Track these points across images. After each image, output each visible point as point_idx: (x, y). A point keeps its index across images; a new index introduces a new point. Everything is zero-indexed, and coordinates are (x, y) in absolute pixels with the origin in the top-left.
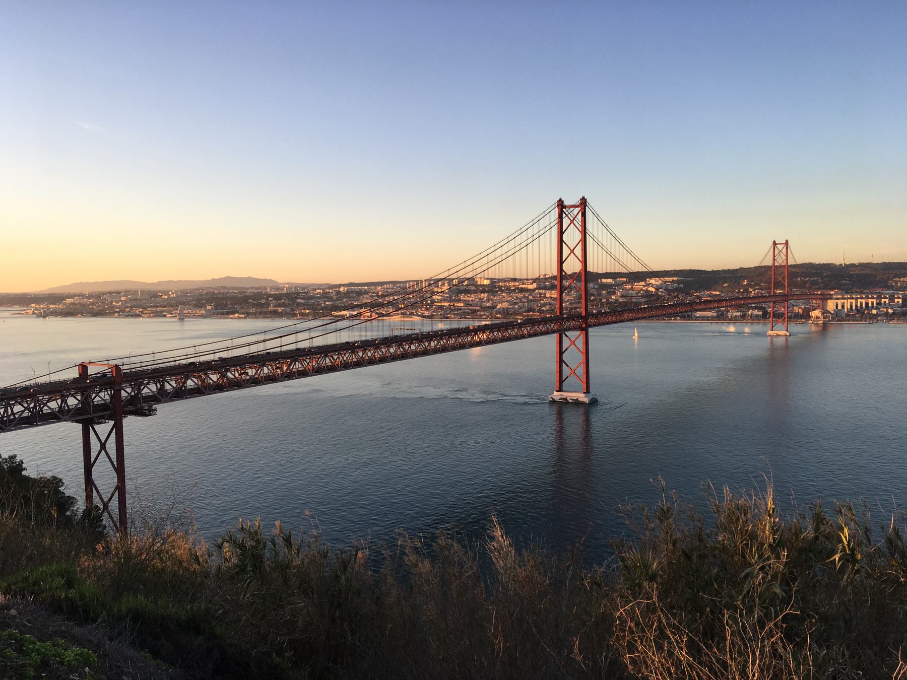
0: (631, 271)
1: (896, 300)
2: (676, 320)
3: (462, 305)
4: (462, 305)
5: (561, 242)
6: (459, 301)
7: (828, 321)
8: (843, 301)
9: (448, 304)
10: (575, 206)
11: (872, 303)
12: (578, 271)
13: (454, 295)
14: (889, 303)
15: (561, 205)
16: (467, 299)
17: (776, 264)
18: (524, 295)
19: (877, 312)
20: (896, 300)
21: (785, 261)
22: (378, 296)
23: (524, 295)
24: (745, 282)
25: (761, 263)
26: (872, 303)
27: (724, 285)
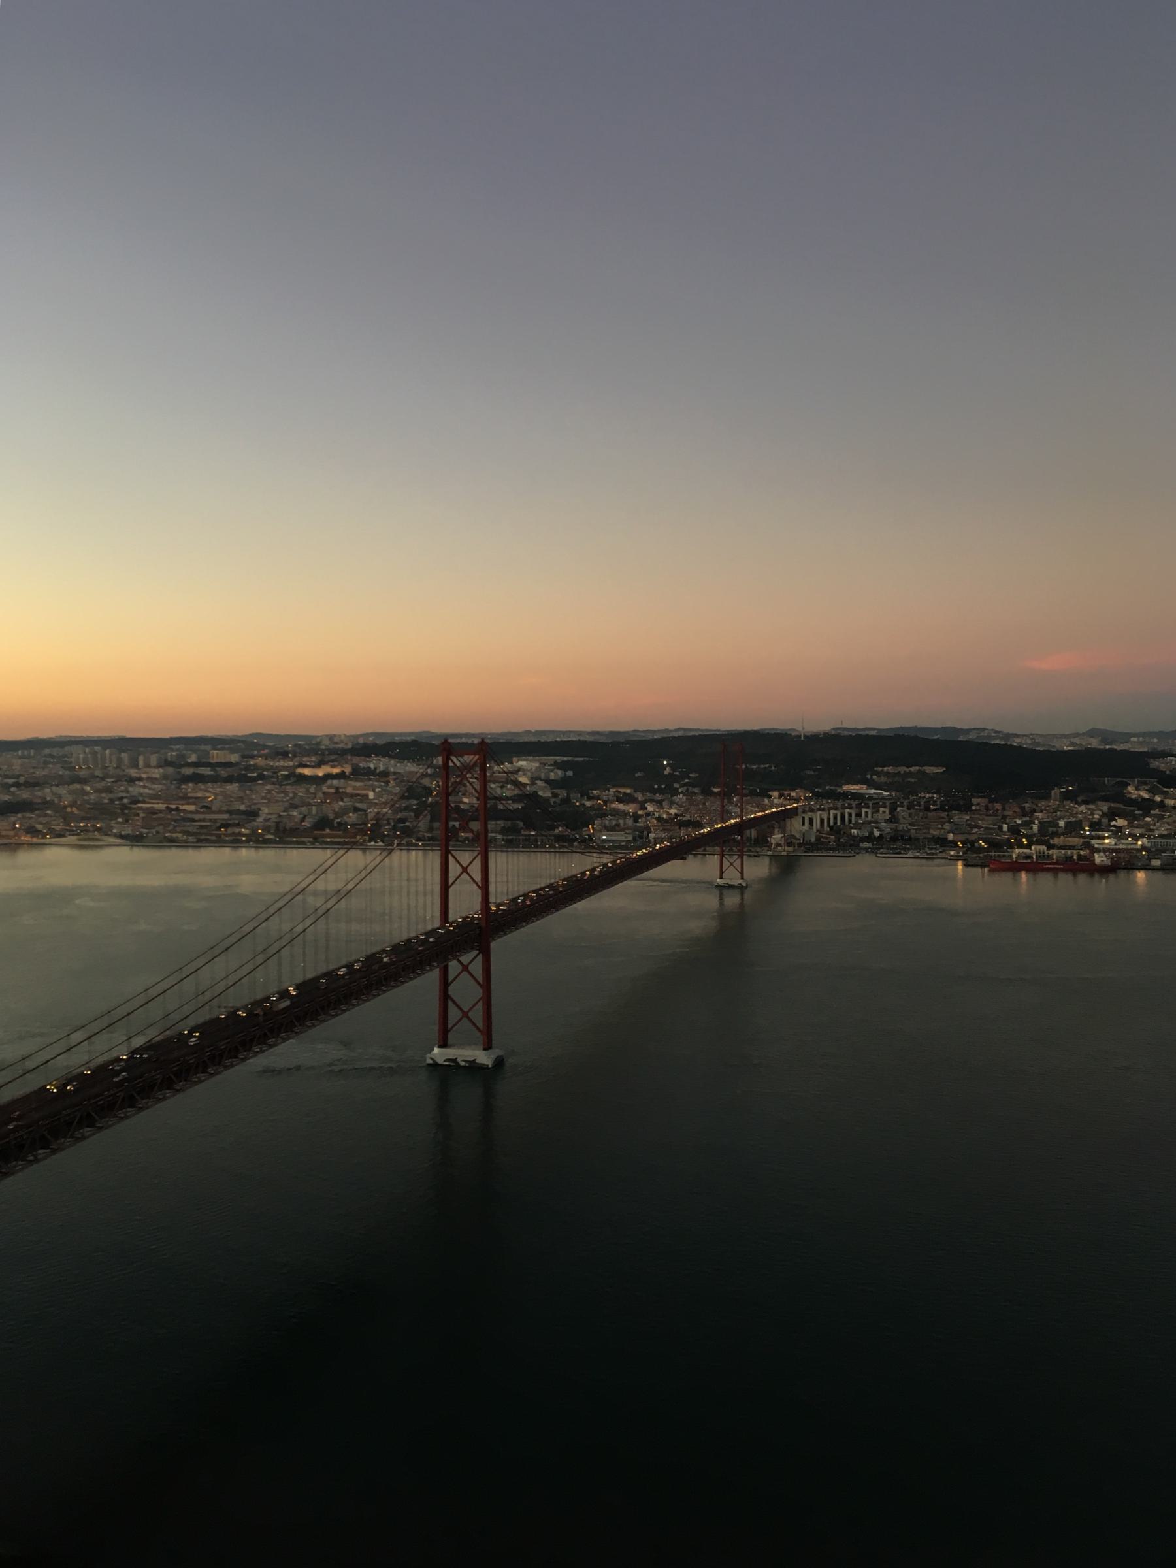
2: (572, 846)
3: (192, 808)
4: (192, 808)
6: (186, 799)
7: (794, 851)
8: (810, 813)
9: (165, 805)
13: (173, 787)
14: (873, 813)
16: (199, 795)
18: (308, 790)
19: (858, 834)
20: (882, 809)
22: (17, 785)
23: (308, 790)
27: (636, 775)
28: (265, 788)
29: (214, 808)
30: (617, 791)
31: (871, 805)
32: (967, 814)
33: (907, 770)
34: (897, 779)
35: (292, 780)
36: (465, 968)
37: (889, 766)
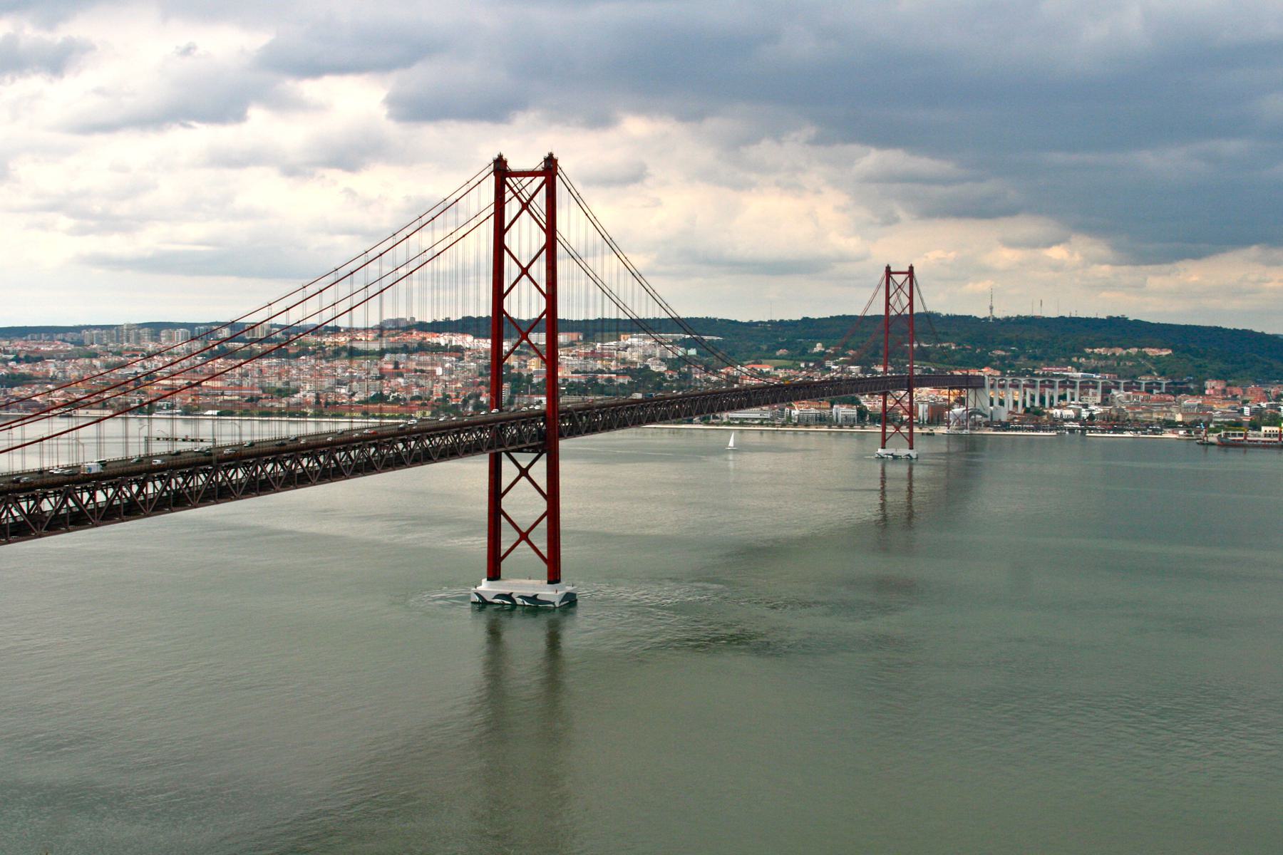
0: (635, 317)
1: (1091, 391)
5: (500, 248)
8: (1000, 391)
9: (186, 382)
10: (533, 174)
11: (1052, 398)
12: (535, 315)
14: (1081, 395)
15: (501, 170)
17: (893, 313)
19: (1061, 414)
21: (907, 311)
22: (18, 360)
24: (819, 347)
25: (866, 310)
26: (1052, 398)
27: (778, 353)
28: (306, 362)
29: (245, 384)
30: (752, 368)
31: (1078, 384)
32: (1198, 398)
33: (1124, 352)
34: (1110, 362)
35: (344, 354)
36: (524, 472)
37: (1101, 347)
